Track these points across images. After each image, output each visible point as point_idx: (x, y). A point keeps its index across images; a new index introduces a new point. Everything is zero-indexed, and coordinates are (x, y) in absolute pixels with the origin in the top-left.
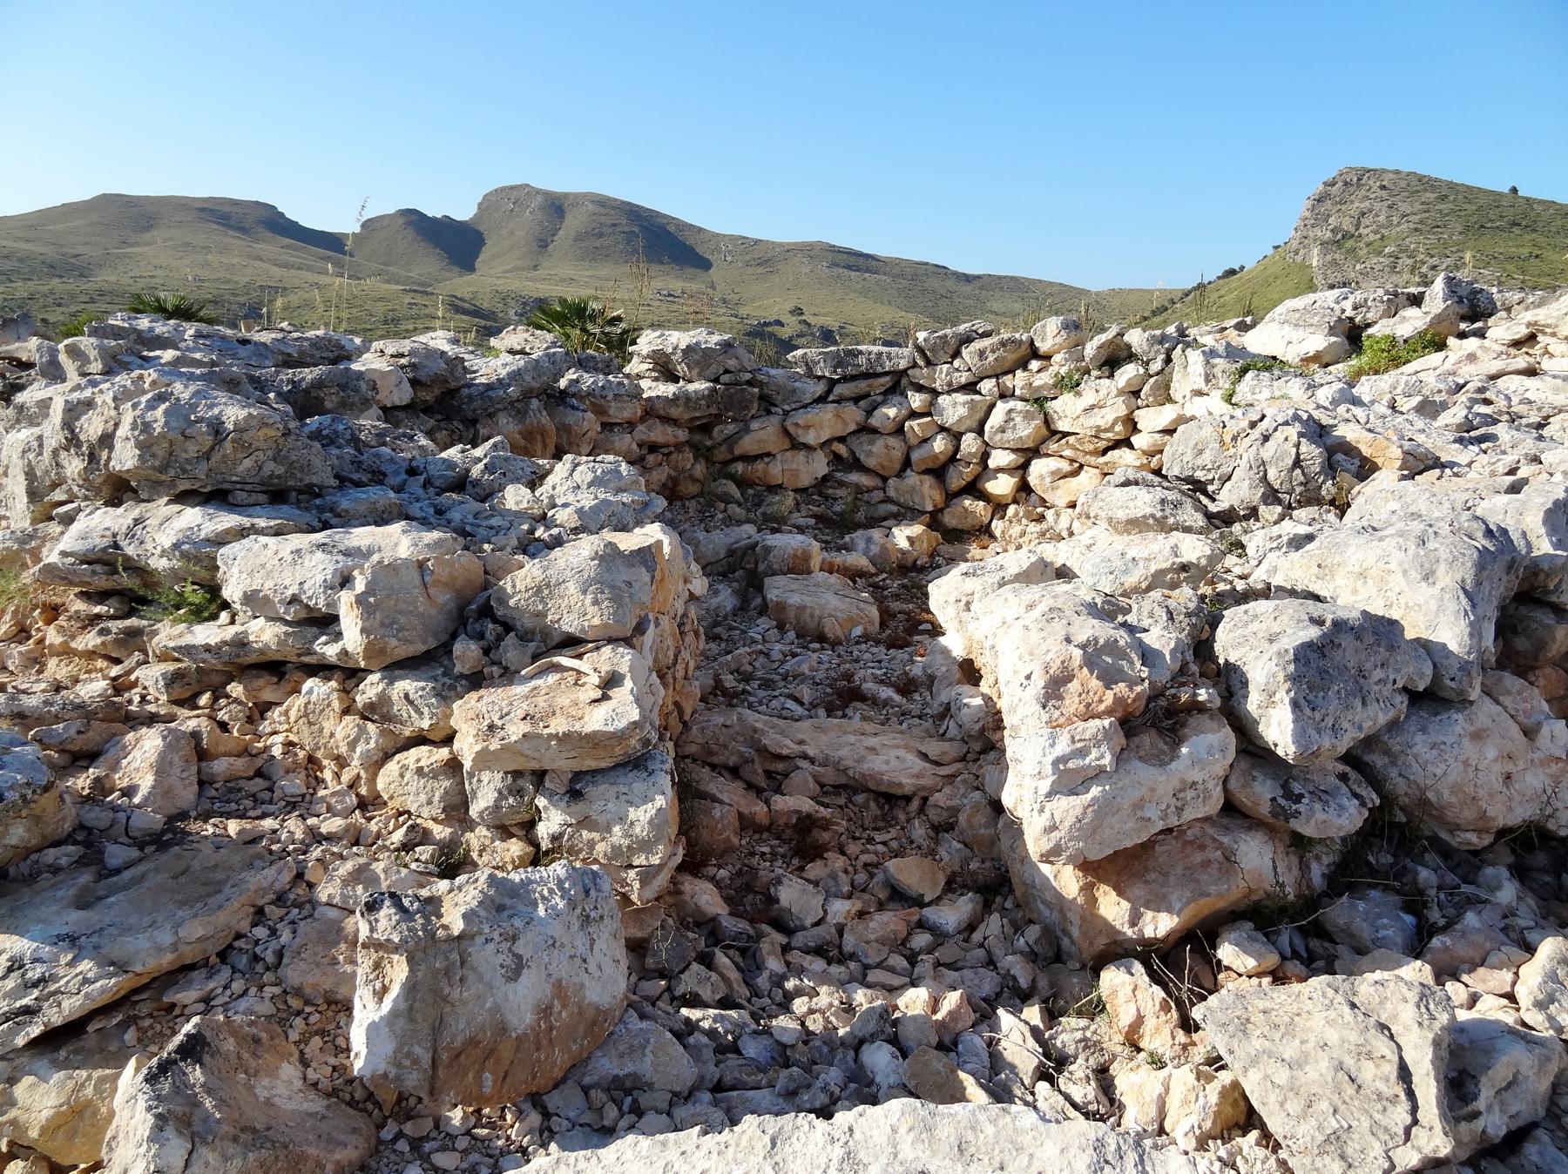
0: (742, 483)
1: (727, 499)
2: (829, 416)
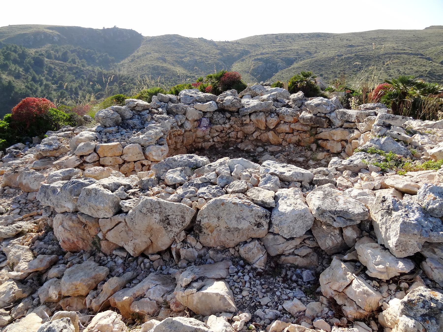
0: (319, 146)
1: (311, 150)
2: (340, 132)
